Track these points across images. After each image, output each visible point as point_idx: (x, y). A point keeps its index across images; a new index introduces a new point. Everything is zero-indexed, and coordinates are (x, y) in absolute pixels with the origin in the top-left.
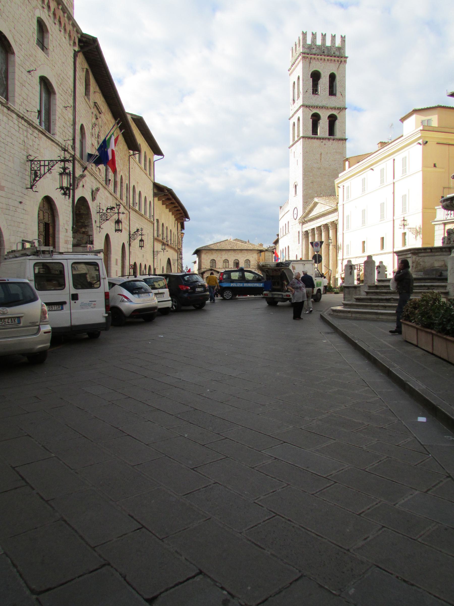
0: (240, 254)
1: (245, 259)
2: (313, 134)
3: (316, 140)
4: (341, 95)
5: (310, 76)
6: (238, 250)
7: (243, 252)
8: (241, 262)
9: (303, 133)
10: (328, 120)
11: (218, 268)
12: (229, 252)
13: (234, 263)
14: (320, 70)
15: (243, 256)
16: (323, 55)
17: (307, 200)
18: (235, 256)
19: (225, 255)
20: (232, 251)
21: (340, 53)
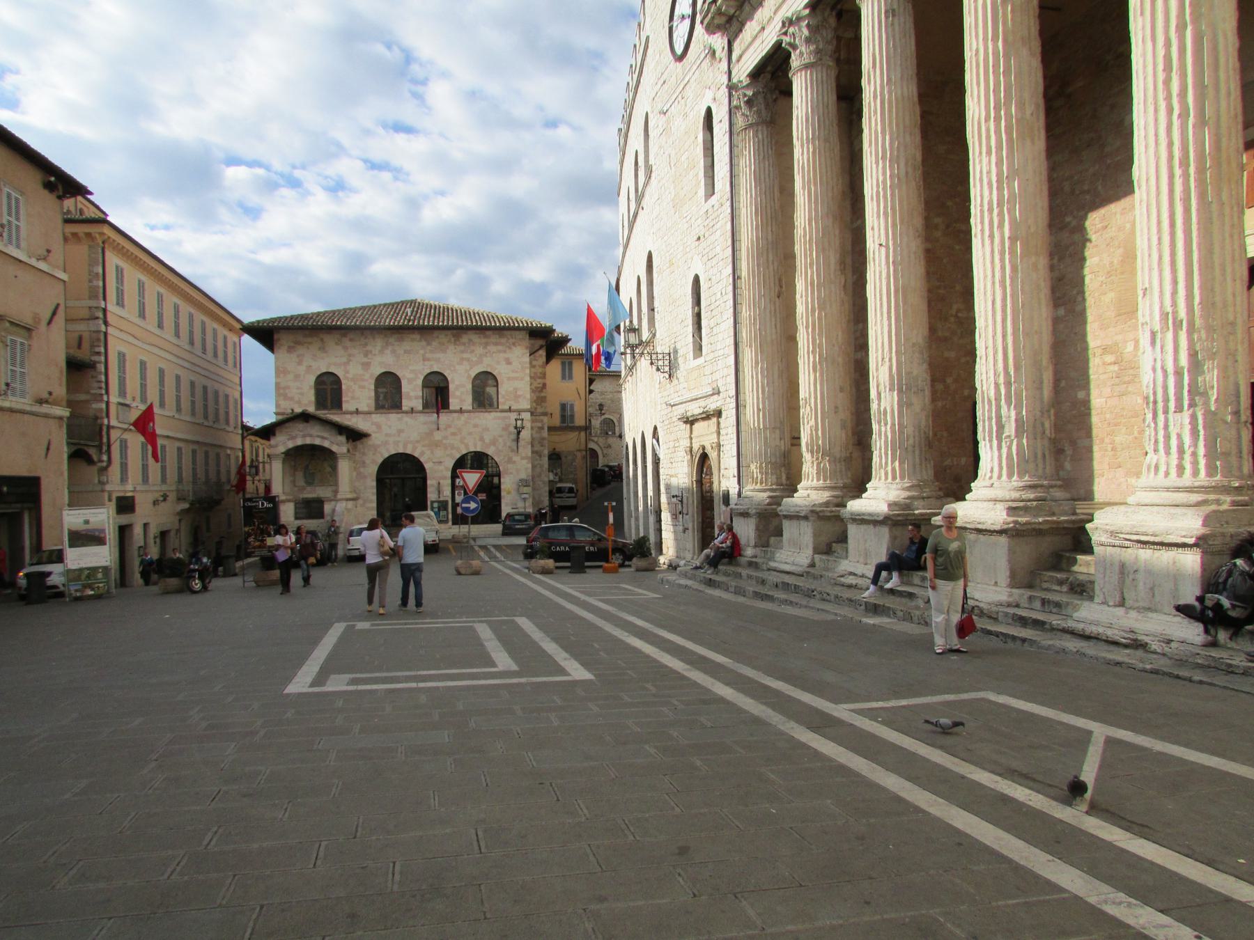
0: (452, 347)
1: (473, 374)
7: (465, 338)
8: (457, 383)
11: (351, 413)
12: (401, 340)
15: (465, 355)
18: (428, 360)
19: (381, 352)
20: (416, 336)
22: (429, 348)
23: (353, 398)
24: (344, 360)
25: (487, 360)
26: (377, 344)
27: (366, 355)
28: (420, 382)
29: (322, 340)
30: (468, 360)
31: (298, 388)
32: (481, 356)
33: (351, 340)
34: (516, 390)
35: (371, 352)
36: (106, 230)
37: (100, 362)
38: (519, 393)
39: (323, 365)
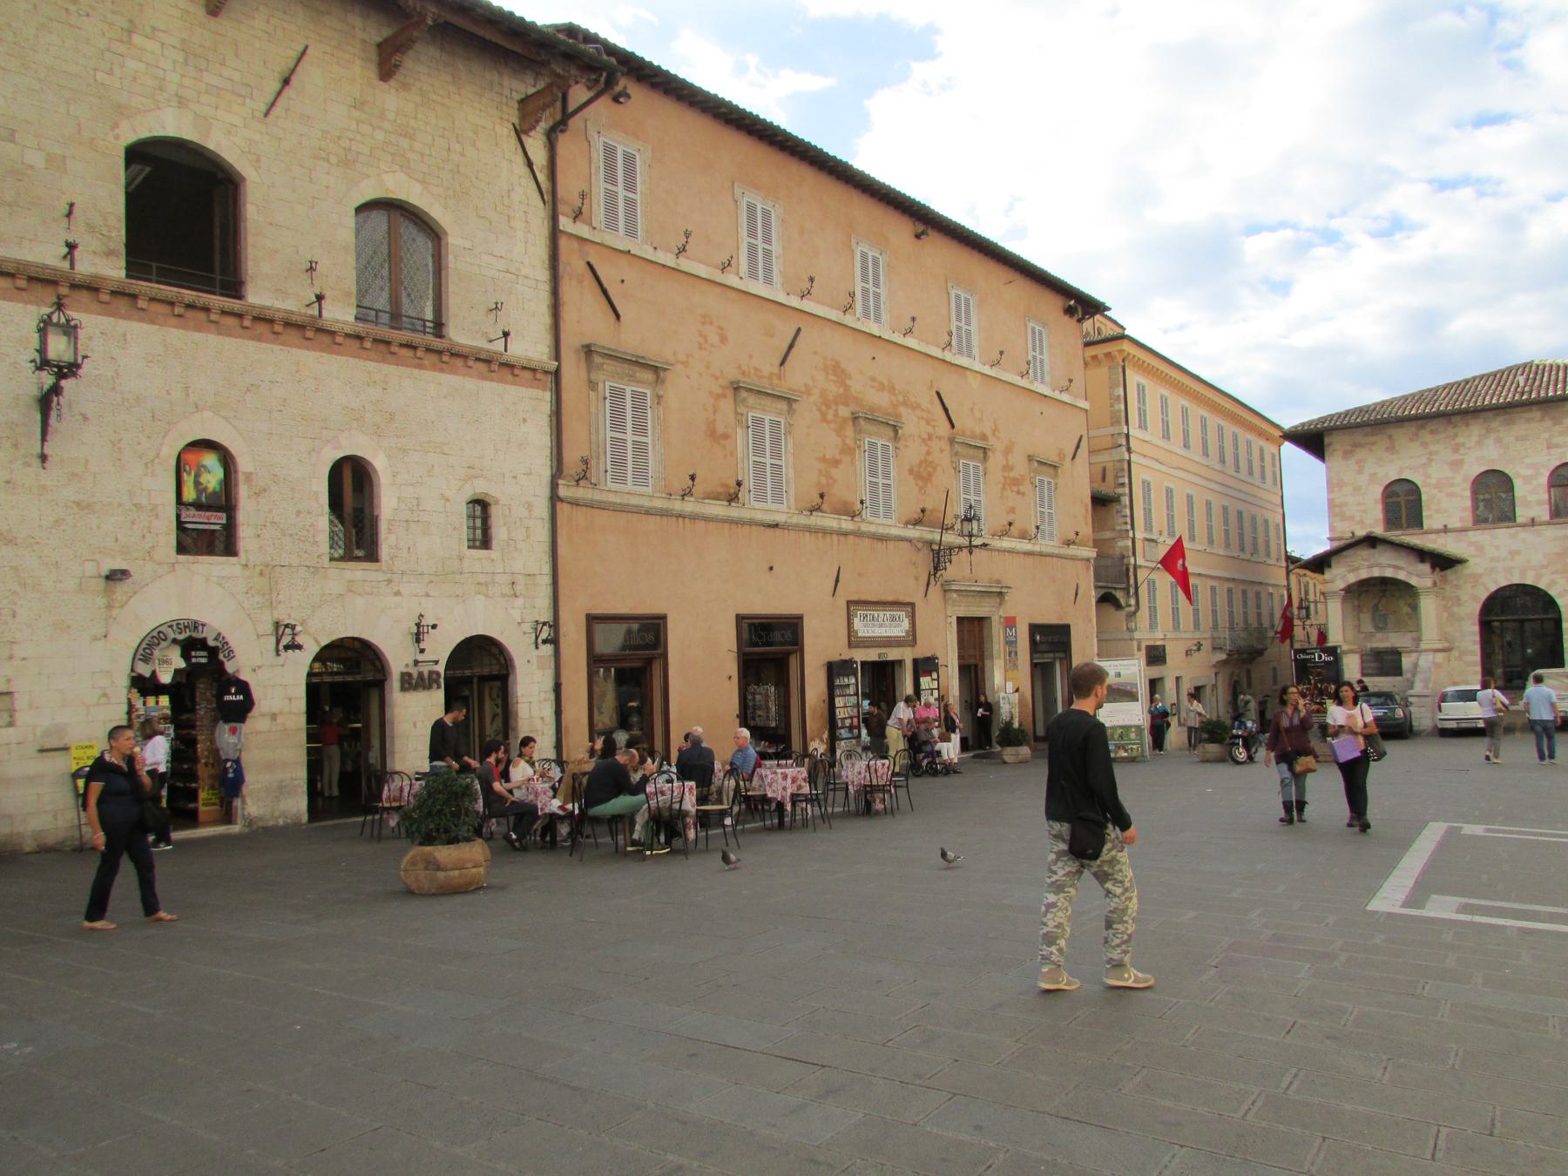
11: (1437, 532)
12: (1510, 423)
18: (1557, 446)
19: (1479, 443)
20: (1536, 414)
22: (1557, 428)
23: (1438, 511)
24: (1424, 460)
26: (1471, 433)
27: (1456, 450)
28: (1544, 480)
29: (1390, 437)
31: (1359, 504)
33: (1432, 432)
35: (1463, 444)
36: (1126, 346)
37: (1125, 495)
39: (1392, 471)
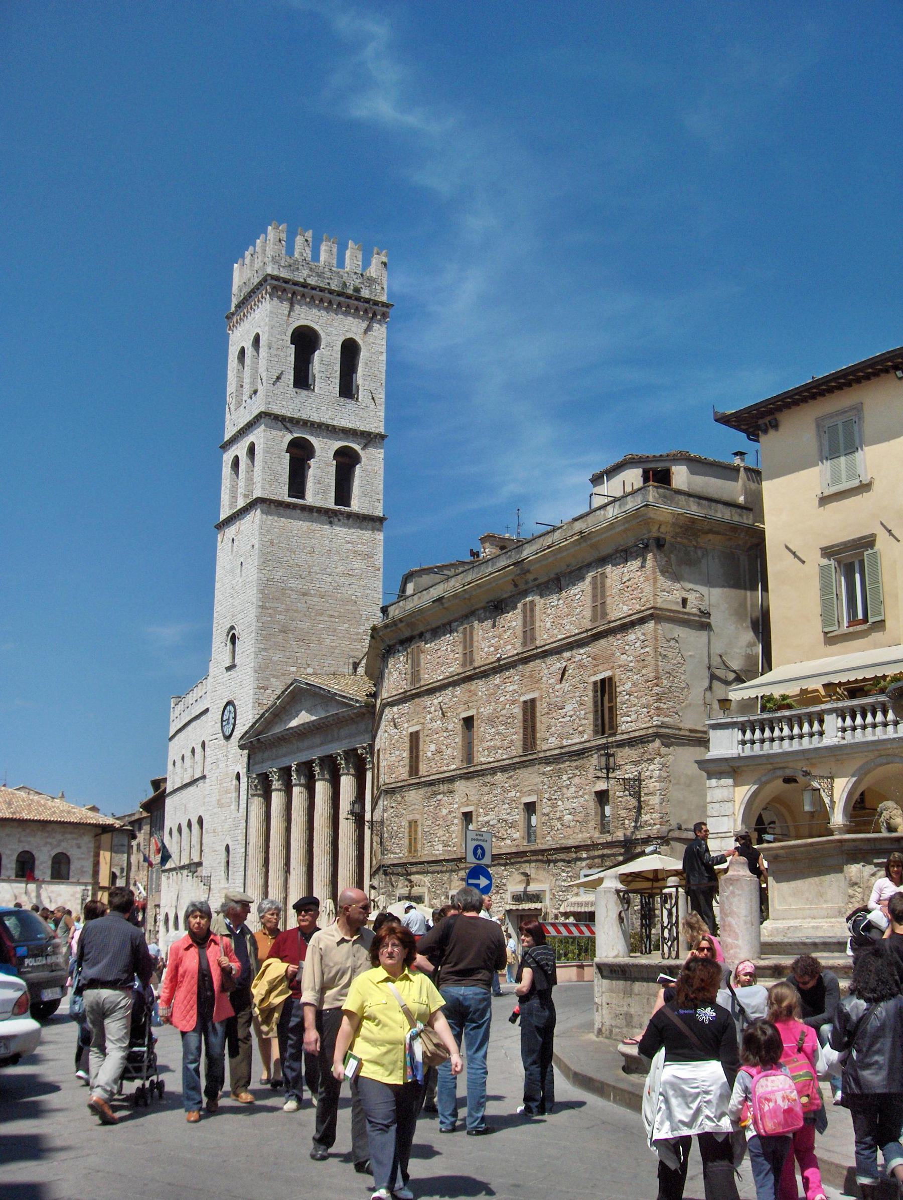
0: (39, 833)
1: (53, 853)
2: (289, 496)
3: (299, 511)
4: (373, 398)
5: (288, 338)
6: (33, 821)
9: (263, 488)
10: (335, 462)
13: (17, 861)
14: (316, 327)
15: (49, 840)
16: (326, 291)
17: (266, 683)
20: (15, 824)
21: (370, 290)
25: (64, 844)
30: (51, 844)
32: (61, 841)
34: (83, 866)
38: (85, 869)
